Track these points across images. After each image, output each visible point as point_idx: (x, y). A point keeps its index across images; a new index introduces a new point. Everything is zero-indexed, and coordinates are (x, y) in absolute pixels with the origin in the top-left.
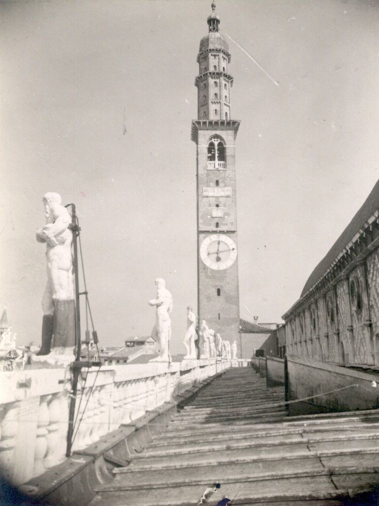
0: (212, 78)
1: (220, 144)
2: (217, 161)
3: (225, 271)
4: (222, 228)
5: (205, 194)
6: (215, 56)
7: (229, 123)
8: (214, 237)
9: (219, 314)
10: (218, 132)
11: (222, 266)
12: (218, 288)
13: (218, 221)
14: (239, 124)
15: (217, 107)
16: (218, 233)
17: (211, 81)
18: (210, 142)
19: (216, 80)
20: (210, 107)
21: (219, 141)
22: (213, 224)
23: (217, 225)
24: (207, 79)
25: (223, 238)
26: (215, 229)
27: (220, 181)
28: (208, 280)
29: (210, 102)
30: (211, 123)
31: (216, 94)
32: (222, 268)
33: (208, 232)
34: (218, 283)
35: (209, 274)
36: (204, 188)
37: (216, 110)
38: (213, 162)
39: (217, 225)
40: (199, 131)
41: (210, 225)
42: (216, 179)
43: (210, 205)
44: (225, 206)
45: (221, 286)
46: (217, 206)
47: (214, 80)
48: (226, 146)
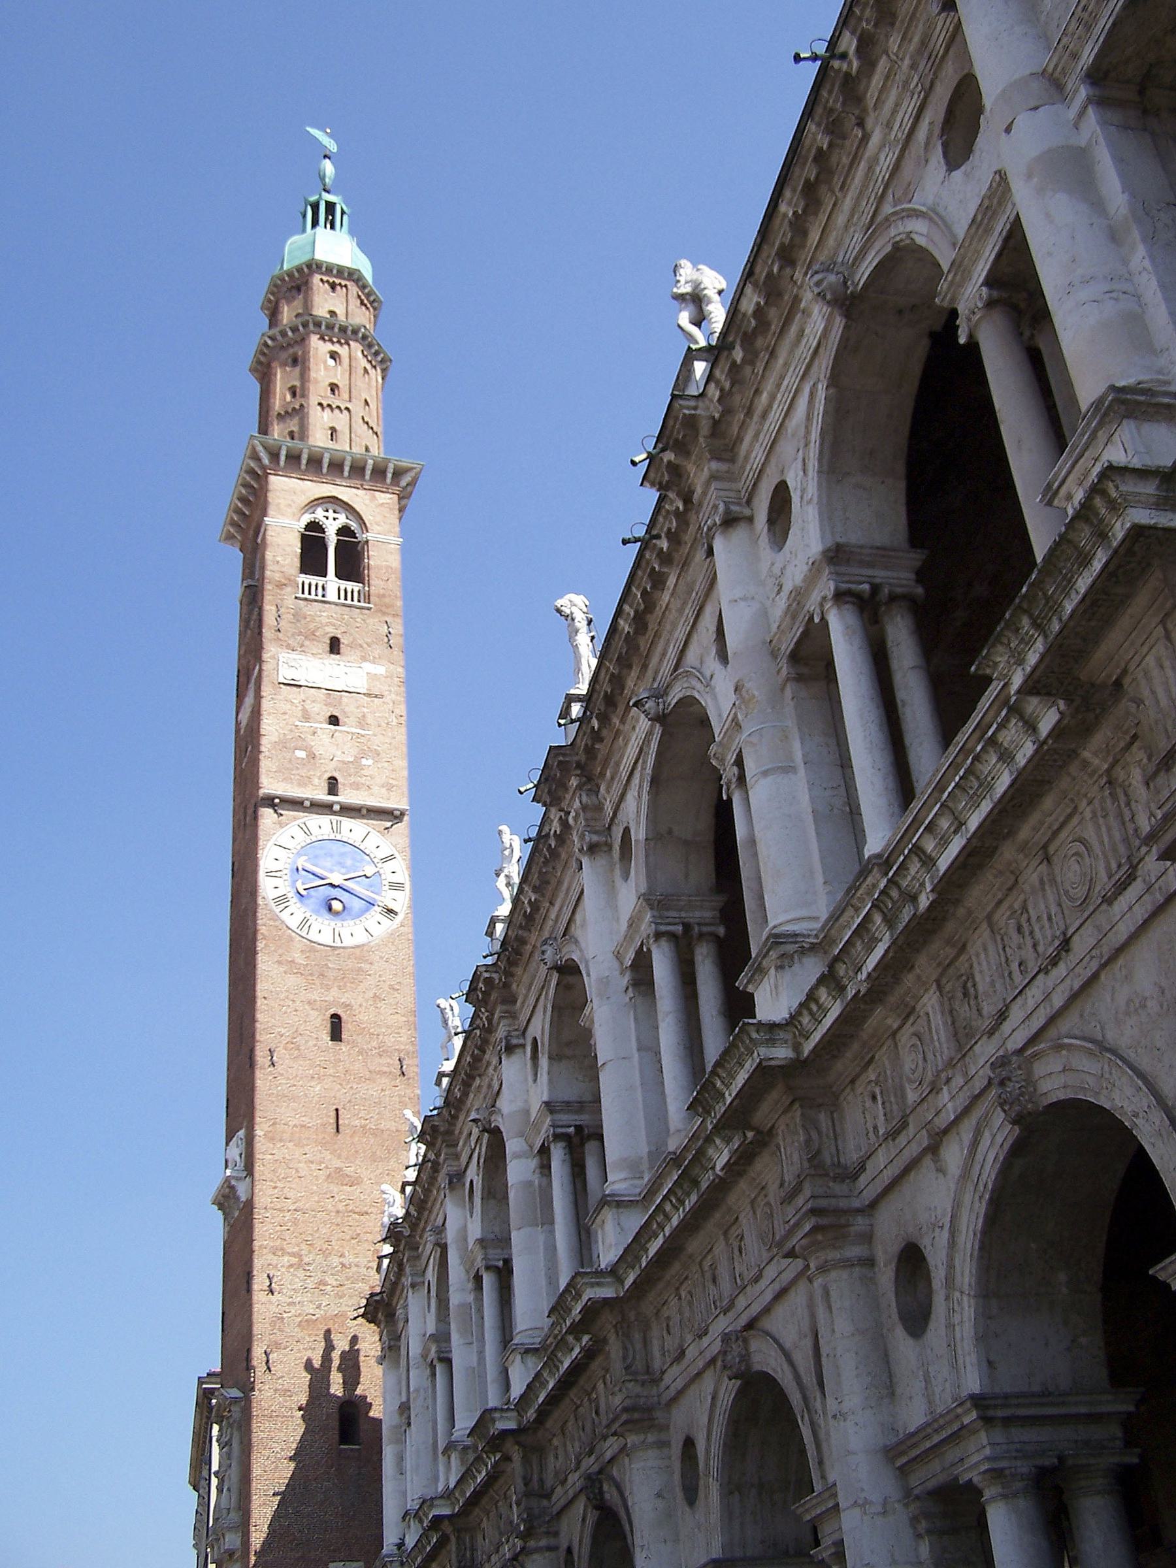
0: (322, 338)
1: (344, 531)
2: (332, 583)
3: (360, 952)
4: (346, 796)
5: (285, 674)
6: (333, 286)
7: (379, 472)
8: (320, 824)
9: (337, 1110)
10: (345, 493)
11: (353, 932)
12: (332, 1011)
13: (336, 775)
14: (413, 483)
15: (340, 421)
16: (335, 813)
17: (319, 348)
18: (307, 518)
19: (336, 348)
20: (312, 420)
21: (342, 519)
22: (316, 781)
23: (333, 785)
24: (303, 341)
25: (354, 829)
26: (323, 796)
27: (344, 640)
28: (292, 980)
29: (313, 400)
30: (315, 462)
31: (334, 388)
32: (348, 942)
33: (296, 804)
34: (334, 993)
35: (300, 959)
36: (284, 656)
37: (333, 430)
38: (320, 580)
39: (333, 785)
40: (272, 478)
41: (304, 782)
42: (332, 632)
43: (306, 717)
44: (362, 722)
45: (347, 1006)
46: (334, 720)
47: (330, 347)
48: (370, 536)
